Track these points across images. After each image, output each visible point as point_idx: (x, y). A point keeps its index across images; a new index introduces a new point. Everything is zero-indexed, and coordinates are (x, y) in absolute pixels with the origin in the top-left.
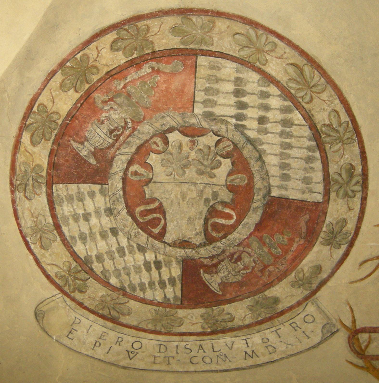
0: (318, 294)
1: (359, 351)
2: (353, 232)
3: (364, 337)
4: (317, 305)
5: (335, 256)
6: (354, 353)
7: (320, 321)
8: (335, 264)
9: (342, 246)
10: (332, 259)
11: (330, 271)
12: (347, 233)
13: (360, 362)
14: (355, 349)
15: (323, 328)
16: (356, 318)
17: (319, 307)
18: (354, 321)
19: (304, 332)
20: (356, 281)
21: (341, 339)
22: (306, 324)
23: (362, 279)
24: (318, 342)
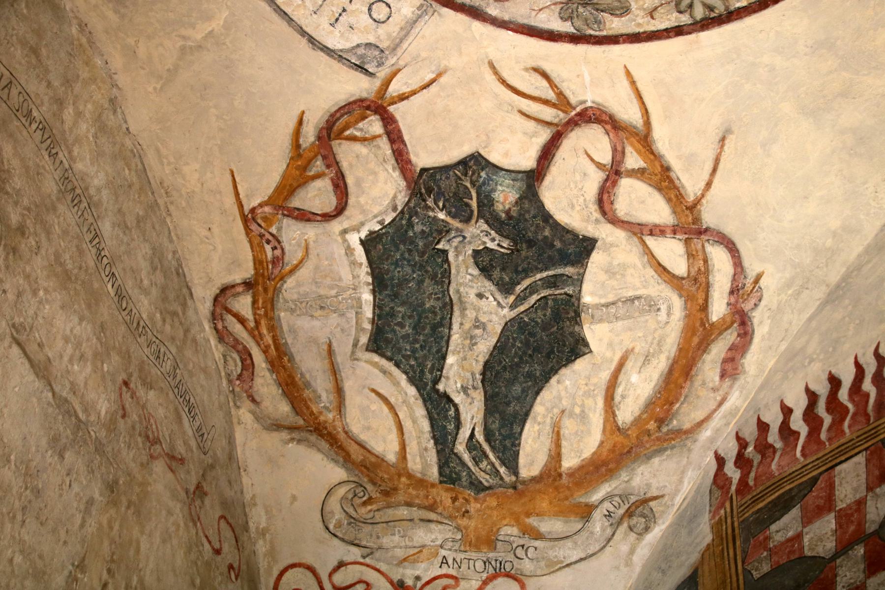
0: (446, 11)
1: (335, 128)
2: (604, 33)
3: (374, 126)
4: (420, 17)
5: (543, 16)
6: (327, 121)
7: (383, 35)
8: (525, 21)
9: (569, 23)
10: (534, 13)
11: (506, 18)
12: (599, 23)
13: (309, 136)
14: (338, 119)
15: (368, 45)
16: (412, 98)
17: (415, 22)
18: (403, 97)
19: (344, 10)
20: (496, 72)
21: (358, 86)
22: (366, 9)
23: (503, 82)
24: (330, 46)
